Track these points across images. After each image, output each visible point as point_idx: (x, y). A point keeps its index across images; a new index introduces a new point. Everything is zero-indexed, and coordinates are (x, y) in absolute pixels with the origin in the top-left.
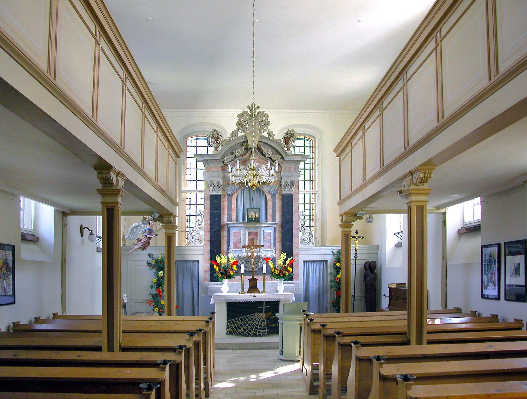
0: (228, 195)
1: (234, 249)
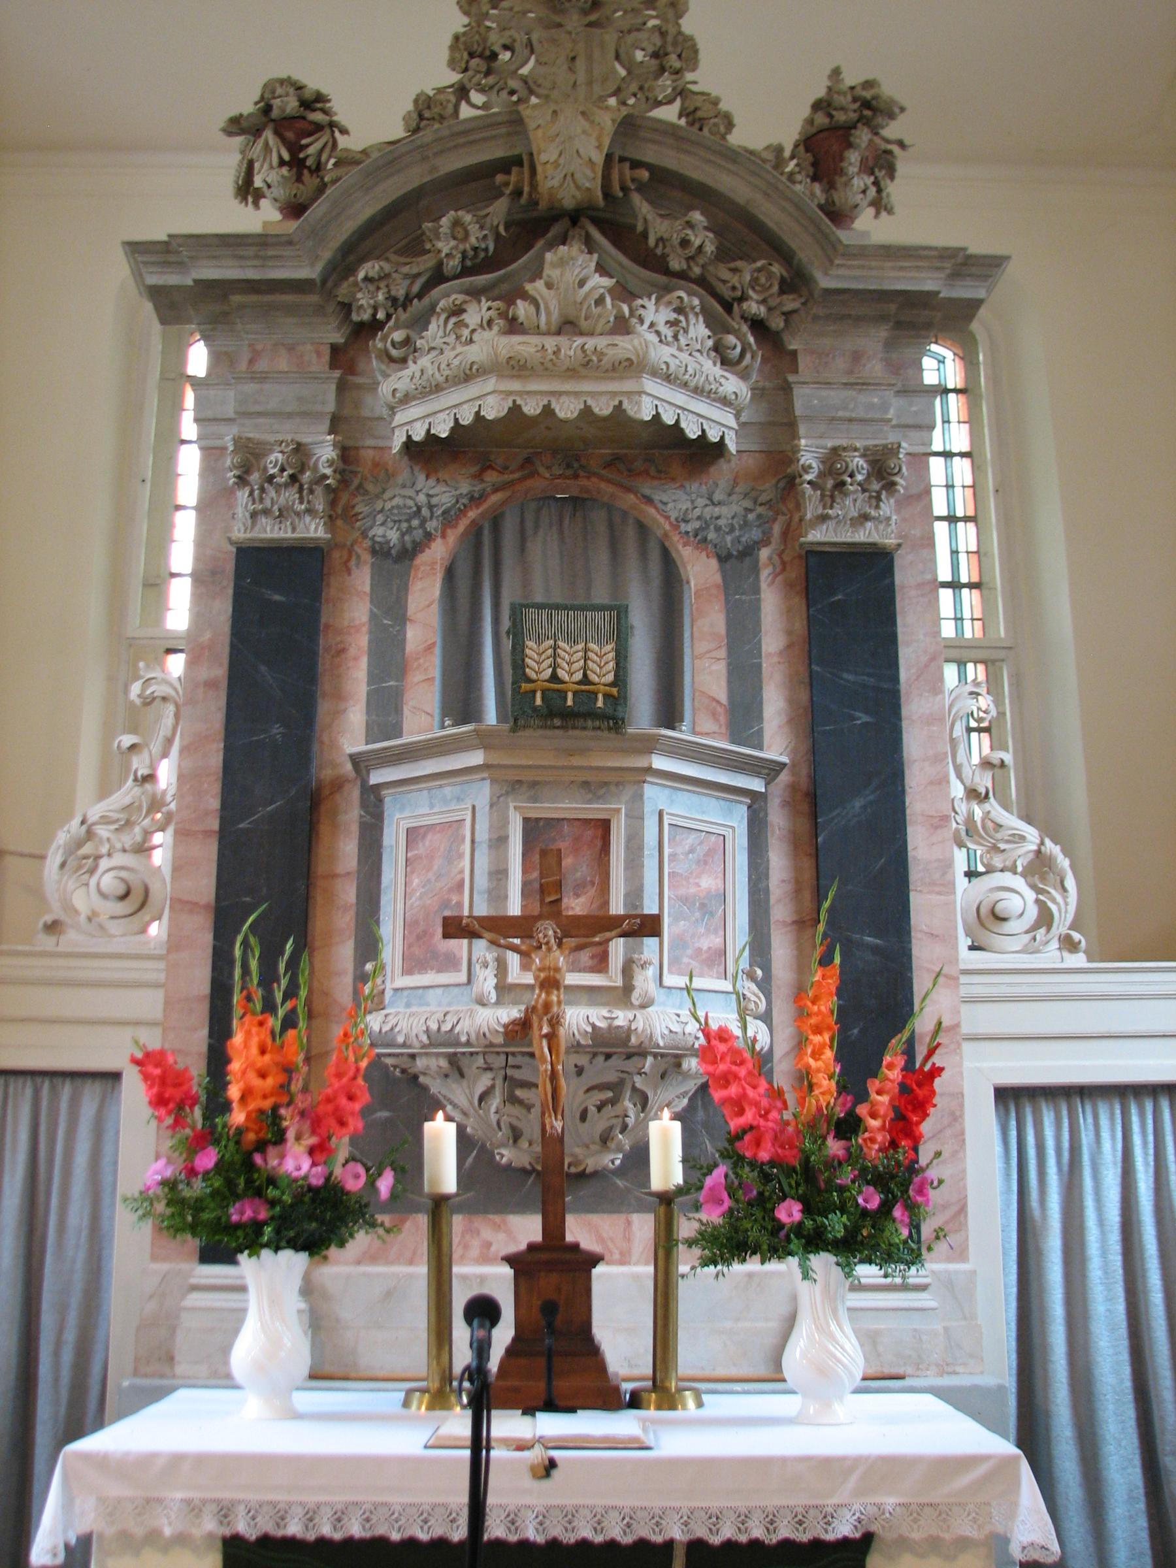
0: (380, 552)
1: (407, 971)
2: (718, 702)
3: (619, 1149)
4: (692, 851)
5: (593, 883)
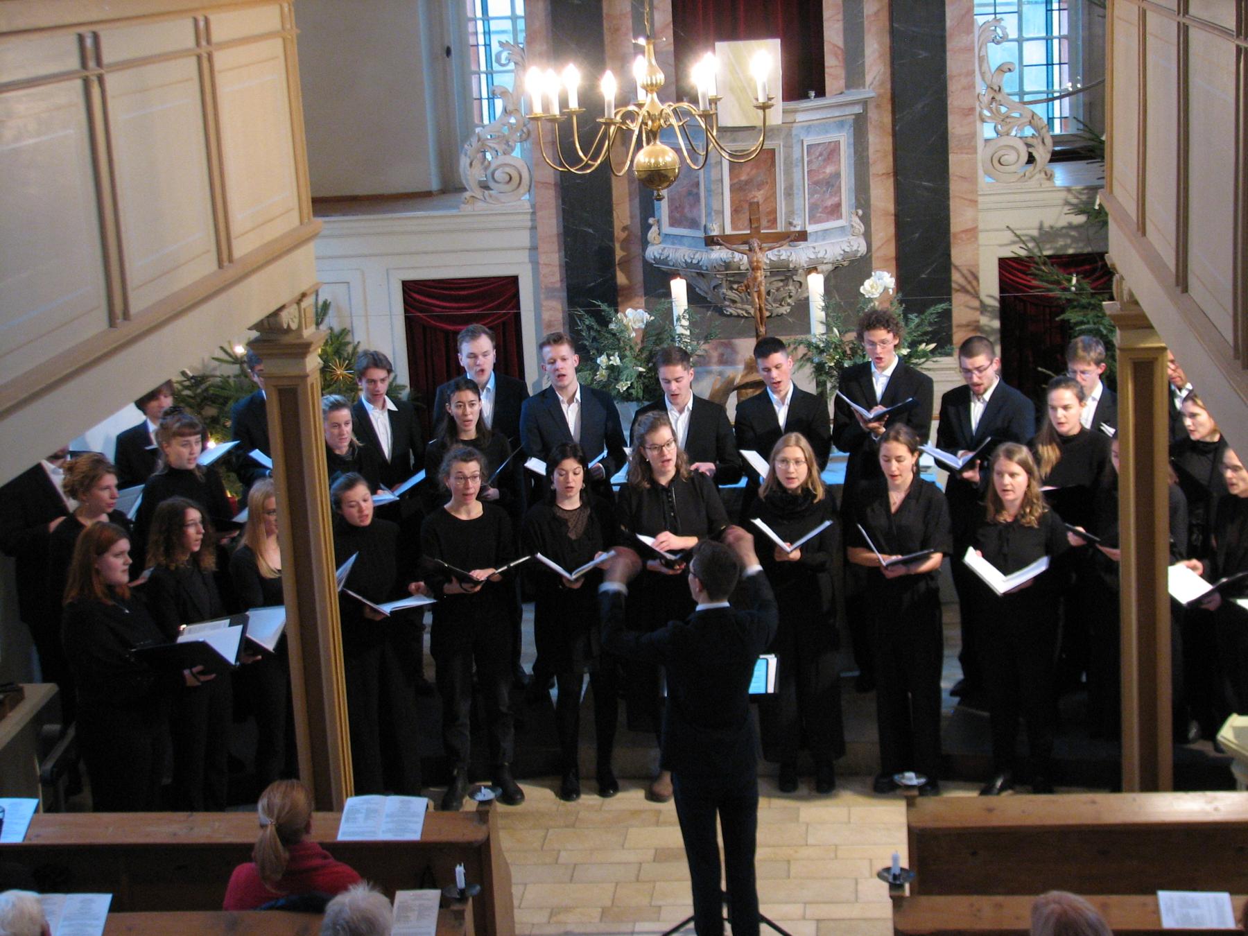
2: (838, 47)
3: (789, 304)
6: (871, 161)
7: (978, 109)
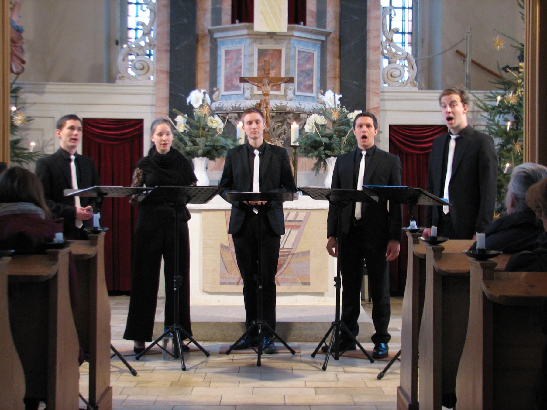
2: (314, 12)
4: (304, 57)
5: (277, 67)
6: (328, 70)
7: (381, 49)
